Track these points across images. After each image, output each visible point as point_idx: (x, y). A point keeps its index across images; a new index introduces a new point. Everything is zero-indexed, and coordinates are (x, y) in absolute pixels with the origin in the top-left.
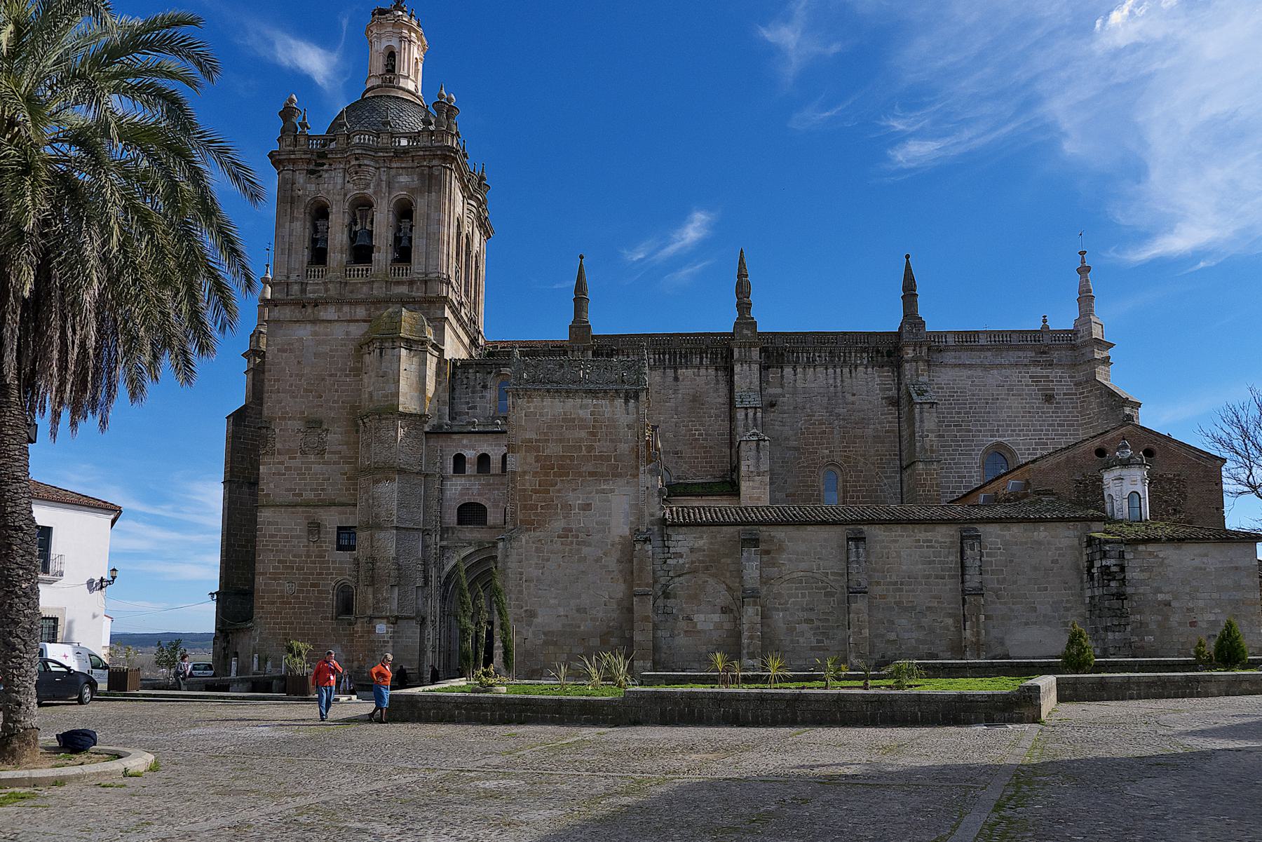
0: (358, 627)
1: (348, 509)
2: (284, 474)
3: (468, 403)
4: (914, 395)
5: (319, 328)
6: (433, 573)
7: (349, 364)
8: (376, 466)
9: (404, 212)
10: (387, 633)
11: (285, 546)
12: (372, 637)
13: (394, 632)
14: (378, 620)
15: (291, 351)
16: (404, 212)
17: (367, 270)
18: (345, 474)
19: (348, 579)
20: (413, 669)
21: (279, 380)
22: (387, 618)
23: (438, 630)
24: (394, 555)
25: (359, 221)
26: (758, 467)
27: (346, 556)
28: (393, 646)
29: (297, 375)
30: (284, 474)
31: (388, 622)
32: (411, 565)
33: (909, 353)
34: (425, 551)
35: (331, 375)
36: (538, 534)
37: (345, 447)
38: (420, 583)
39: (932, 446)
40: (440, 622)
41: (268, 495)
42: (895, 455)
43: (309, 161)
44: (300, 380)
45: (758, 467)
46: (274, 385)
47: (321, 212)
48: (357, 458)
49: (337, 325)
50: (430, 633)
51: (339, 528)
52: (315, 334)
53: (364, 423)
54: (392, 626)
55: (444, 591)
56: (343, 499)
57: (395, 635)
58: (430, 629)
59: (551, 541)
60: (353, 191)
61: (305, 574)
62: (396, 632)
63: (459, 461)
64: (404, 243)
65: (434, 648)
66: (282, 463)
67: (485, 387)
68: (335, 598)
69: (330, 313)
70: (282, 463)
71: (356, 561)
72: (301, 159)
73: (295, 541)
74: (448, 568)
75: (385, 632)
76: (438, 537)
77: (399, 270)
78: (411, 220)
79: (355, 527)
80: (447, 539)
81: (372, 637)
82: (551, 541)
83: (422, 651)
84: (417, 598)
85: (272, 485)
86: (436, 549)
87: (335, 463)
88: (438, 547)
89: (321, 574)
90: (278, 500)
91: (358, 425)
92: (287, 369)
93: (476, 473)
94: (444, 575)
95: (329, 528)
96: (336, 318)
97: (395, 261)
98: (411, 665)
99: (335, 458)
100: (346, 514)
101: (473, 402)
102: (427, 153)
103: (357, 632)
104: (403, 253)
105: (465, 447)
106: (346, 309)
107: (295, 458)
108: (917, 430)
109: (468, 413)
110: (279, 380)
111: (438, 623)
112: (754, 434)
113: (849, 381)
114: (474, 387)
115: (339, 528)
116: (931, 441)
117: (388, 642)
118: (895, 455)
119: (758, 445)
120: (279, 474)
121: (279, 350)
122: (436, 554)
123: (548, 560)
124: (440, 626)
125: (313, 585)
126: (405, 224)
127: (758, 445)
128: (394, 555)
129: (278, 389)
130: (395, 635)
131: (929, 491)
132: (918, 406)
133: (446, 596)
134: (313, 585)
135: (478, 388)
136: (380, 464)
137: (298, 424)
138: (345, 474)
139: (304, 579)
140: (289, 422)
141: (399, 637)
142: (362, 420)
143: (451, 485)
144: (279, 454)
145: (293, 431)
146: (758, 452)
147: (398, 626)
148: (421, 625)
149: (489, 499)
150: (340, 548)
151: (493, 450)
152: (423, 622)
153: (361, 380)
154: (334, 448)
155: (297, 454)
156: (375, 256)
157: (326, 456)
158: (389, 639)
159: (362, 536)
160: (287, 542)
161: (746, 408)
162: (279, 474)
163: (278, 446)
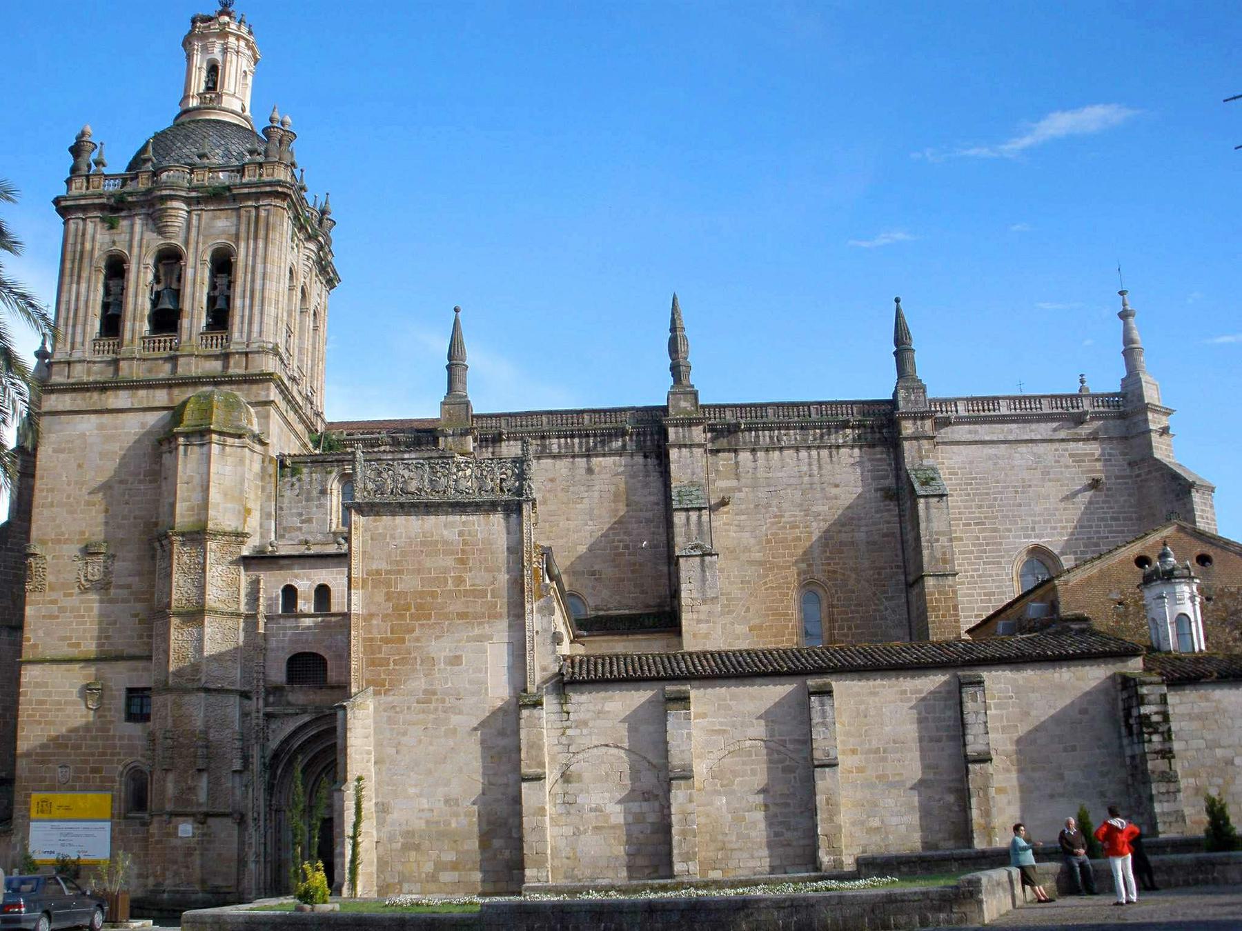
0: (154, 829)
1: (140, 664)
2: (57, 617)
3: (301, 515)
4: (917, 486)
5: (106, 418)
6: (256, 752)
7: (144, 465)
9: (223, 264)
10: (193, 837)
11: (57, 716)
13: (204, 835)
14: (180, 819)
15: (71, 451)
16: (223, 264)
17: (171, 340)
18: (136, 615)
19: (139, 760)
21: (52, 490)
22: (193, 815)
23: (262, 832)
25: (162, 278)
26: (703, 592)
27: (136, 729)
28: (202, 855)
29: (76, 483)
30: (57, 617)
31: (195, 821)
32: (225, 741)
33: (908, 428)
35: (121, 482)
36: (390, 699)
37: (137, 579)
38: (237, 765)
39: (944, 554)
40: (266, 820)
41: (35, 646)
42: (898, 567)
43: (102, 207)
44: (80, 489)
45: (703, 592)
46: (46, 497)
47: (116, 268)
48: (152, 594)
49: (131, 415)
50: (254, 836)
51: (130, 691)
52: (101, 427)
53: (162, 546)
57: (206, 839)
58: (251, 830)
59: (409, 708)
60: (156, 242)
61: (84, 754)
63: (290, 594)
64: (220, 304)
65: (258, 856)
66: (54, 602)
68: (123, 787)
69: (121, 399)
70: (54, 602)
71: (151, 737)
72: (93, 204)
73: (70, 709)
74: (274, 744)
76: (261, 702)
77: (212, 340)
78: (230, 274)
79: (150, 689)
80: (273, 704)
81: (174, 842)
82: (409, 708)
83: (242, 862)
85: (41, 633)
86: (257, 718)
87: (124, 601)
88: (261, 715)
89: (104, 754)
90: (48, 655)
91: (154, 549)
92: (64, 475)
93: (313, 611)
94: (269, 753)
95: (117, 690)
96: (129, 406)
97: (210, 327)
99: (124, 593)
101: (308, 513)
102: (253, 190)
103: (153, 835)
104: (219, 318)
105: (296, 577)
106: (142, 393)
107: (71, 595)
108: (922, 532)
109: (300, 529)
110: (52, 490)
111: (262, 823)
112: (697, 547)
113: (829, 467)
114: (309, 492)
115: (130, 691)
116: (943, 547)
118: (898, 567)
119: (703, 562)
120: (52, 617)
121: (55, 451)
122: (258, 725)
123: (405, 734)
124: (265, 826)
125: (94, 770)
126: (222, 280)
127: (703, 562)
129: (52, 502)
131: (944, 616)
132: (922, 500)
134: (94, 770)
135: (315, 493)
137: (74, 549)
138: (136, 615)
139: (86, 762)
140: (65, 546)
141: (209, 842)
142: (160, 541)
143: (278, 628)
144: (52, 589)
145: (69, 557)
146: (703, 571)
147: (209, 827)
150: (131, 717)
151: (335, 579)
152: (241, 821)
153: (160, 487)
154: (122, 581)
155: (74, 588)
156: (185, 322)
157: (112, 591)
159: (157, 700)
160: (58, 710)
161: (687, 510)
162: (52, 617)
163: (50, 578)
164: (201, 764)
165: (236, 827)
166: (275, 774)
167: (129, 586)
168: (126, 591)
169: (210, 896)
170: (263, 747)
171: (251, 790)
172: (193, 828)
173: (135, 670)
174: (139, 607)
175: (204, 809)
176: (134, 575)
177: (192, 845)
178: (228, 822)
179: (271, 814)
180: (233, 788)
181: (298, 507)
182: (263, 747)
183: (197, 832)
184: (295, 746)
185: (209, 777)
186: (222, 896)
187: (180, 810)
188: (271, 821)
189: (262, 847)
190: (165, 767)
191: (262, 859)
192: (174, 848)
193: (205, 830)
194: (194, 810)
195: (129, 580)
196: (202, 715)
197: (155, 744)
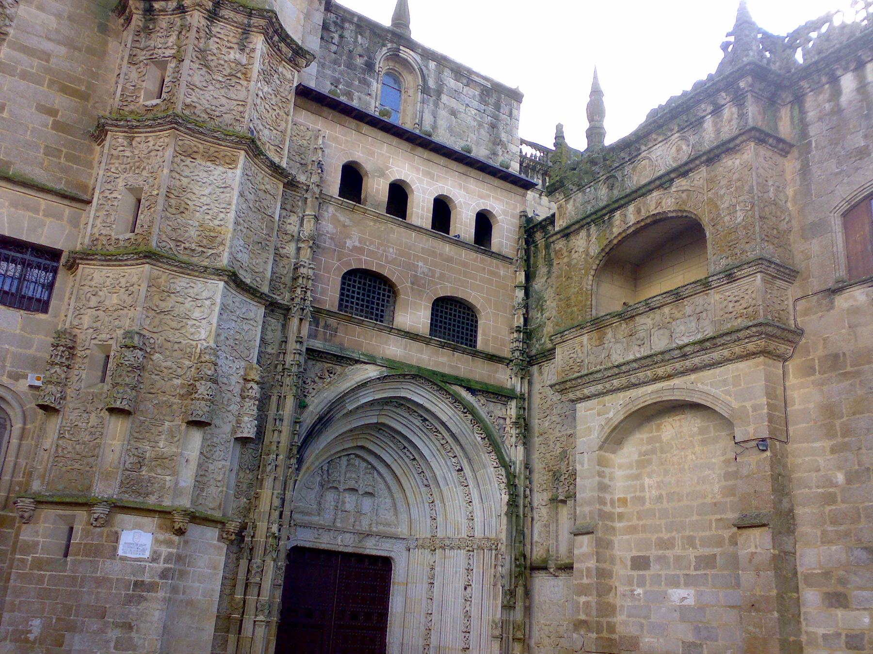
1: (44, 202)
8: (187, 112)
10: (154, 559)
12: (109, 568)
14: (128, 519)
18: (52, 112)
22: (164, 513)
24: (212, 344)
37: (63, 50)
54: (176, 538)
56: (39, 175)
67: (370, 66)
75: (147, 555)
81: (109, 568)
87: (24, 75)
88: (304, 350)
94: (309, 418)
100: (37, 211)
117: (152, 587)
128: (212, 344)
135: (359, 61)
136: (197, 112)
138: (52, 112)
154: (33, 42)
158: (157, 580)
164: (201, 410)
167: (46, 56)
168: (36, 62)
170: (302, 406)
172: (156, 541)
173: (27, 208)
174: (59, 101)
175: (185, 502)
176: (59, 43)
177: (147, 579)
178: (211, 534)
181: (334, 70)
182: (302, 406)
183: (164, 550)
187: (129, 499)
190: (118, 405)
192: (102, 582)
194: (167, 503)
195: (48, 46)
197: (72, 356)
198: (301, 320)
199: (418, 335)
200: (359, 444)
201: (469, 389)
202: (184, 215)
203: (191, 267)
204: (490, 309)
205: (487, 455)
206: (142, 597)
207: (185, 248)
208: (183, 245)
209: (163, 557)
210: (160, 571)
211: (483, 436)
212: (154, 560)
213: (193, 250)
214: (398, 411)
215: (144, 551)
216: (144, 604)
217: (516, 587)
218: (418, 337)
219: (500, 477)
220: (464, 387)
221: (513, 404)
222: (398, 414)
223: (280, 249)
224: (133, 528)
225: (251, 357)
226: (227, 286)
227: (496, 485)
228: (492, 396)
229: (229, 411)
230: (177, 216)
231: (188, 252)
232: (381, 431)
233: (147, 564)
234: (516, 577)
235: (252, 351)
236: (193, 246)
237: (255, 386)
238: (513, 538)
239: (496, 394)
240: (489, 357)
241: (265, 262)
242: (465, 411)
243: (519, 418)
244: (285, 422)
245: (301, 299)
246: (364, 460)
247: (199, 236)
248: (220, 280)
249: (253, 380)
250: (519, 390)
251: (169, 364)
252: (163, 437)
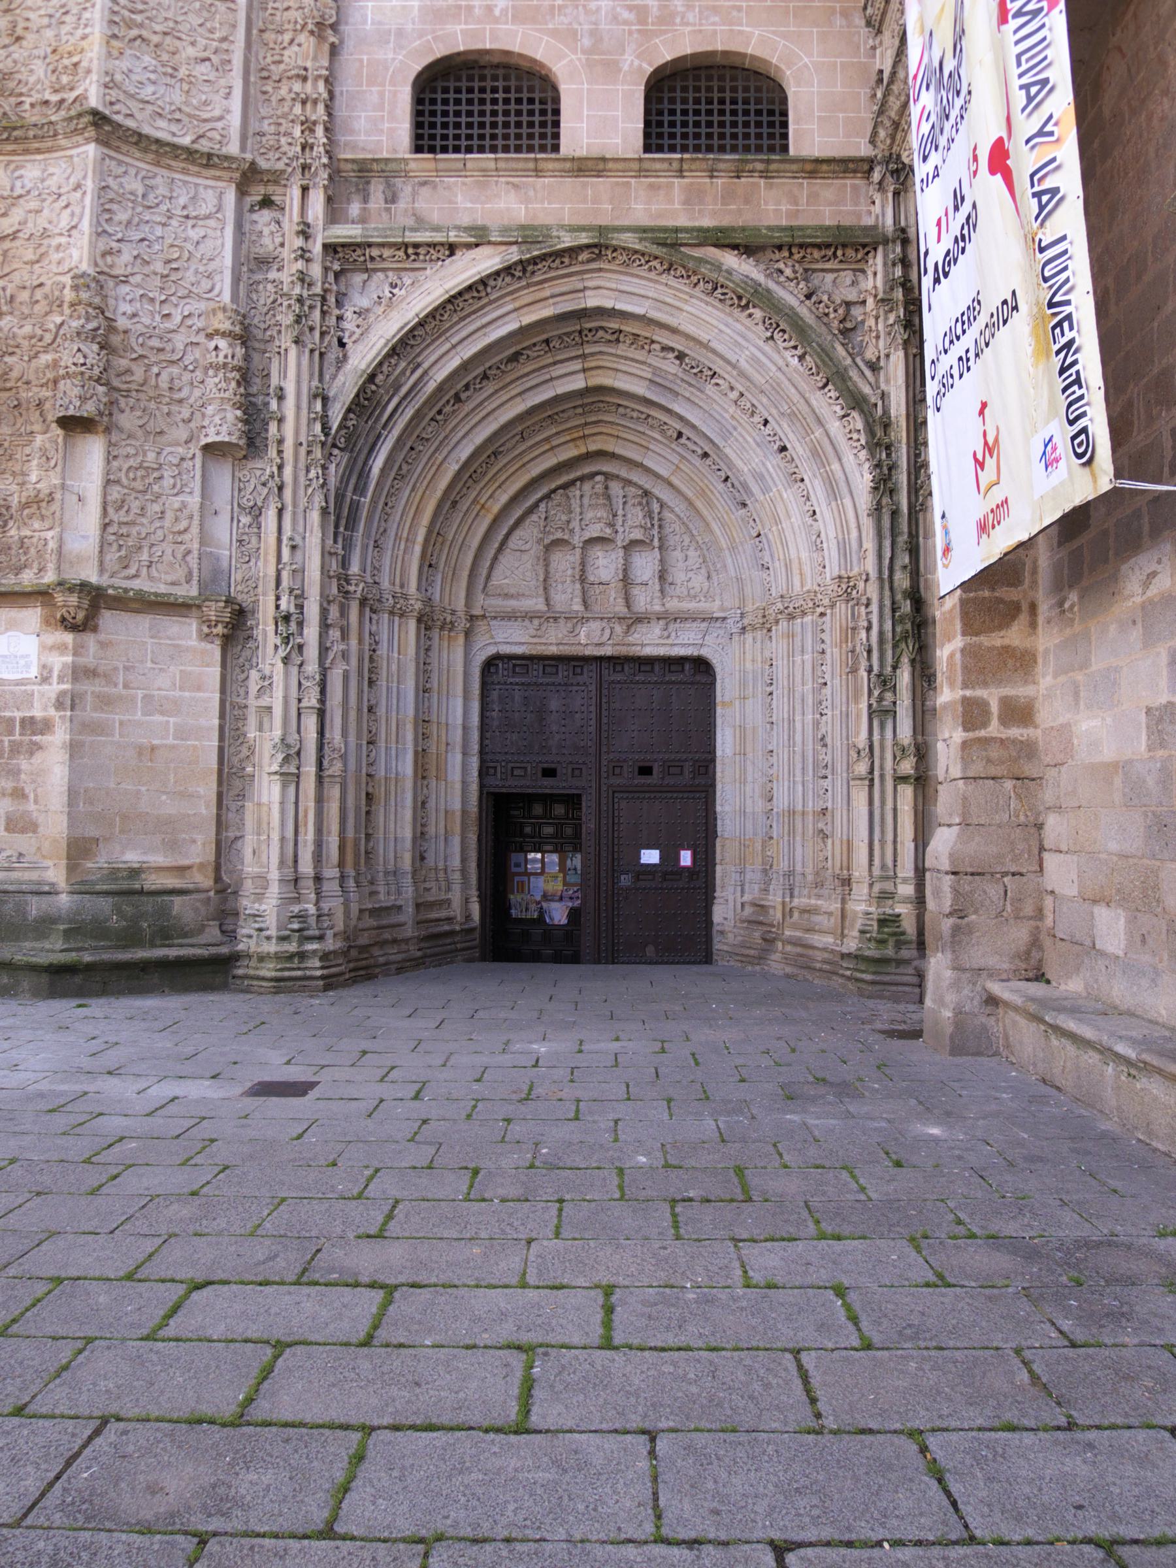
20: (182, 870)
22: (42, 595)
23: (312, 668)
28: (74, 749)
32: (180, 341)
34: (253, 286)
40: (325, 626)
54: (68, 638)
55: (344, 480)
62: (91, 673)
65: (292, 755)
75: (34, 672)
76: (317, 200)
84: (207, 510)
88: (317, 249)
98: (172, 845)
111: (311, 633)
117: (46, 726)
124: (323, 650)
130: (90, 688)
133: (355, 508)
141: (105, 702)
148: (228, 641)
149: (570, 36)
158: (52, 712)
165: (215, 650)
166: (364, 475)
169: (104, 905)
171: (270, 516)
172: (44, 648)
177: (37, 713)
179: (344, 612)
180: (207, 510)
184: (440, 375)
185: (110, 458)
186: (148, 904)
188: (345, 636)
189: (311, 723)
191: (310, 769)
193: (89, 659)
196: (85, 225)
198: (305, 189)
199: (604, 159)
200: (593, 447)
201: (747, 249)
202: (24, 43)
203: (31, 133)
204: (810, 55)
205: (819, 393)
206: (35, 744)
207: (32, 105)
208: (28, 100)
209: (55, 674)
210: (53, 696)
211: (799, 352)
212: (45, 680)
213: (46, 102)
214: (621, 350)
215: (28, 666)
216: (38, 758)
217: (895, 668)
218: (610, 165)
219: (855, 436)
220: (735, 247)
221: (878, 261)
222: (626, 358)
223: (273, 67)
224: (7, 630)
225: (216, 291)
226: (106, 151)
227: (852, 457)
228: (817, 254)
229: (180, 401)
230: (12, 48)
231: (38, 108)
232: (621, 410)
233: (35, 688)
234: (895, 646)
235: (217, 278)
236: (48, 96)
237: (223, 343)
238: (886, 562)
239: (828, 246)
240: (809, 167)
241: (228, 96)
242: (744, 302)
243: (892, 289)
244: (290, 401)
245: (303, 148)
246: (629, 482)
247: (54, 71)
248: (88, 141)
249: (217, 332)
250: (889, 221)
251: (27, 329)
252: (35, 462)
